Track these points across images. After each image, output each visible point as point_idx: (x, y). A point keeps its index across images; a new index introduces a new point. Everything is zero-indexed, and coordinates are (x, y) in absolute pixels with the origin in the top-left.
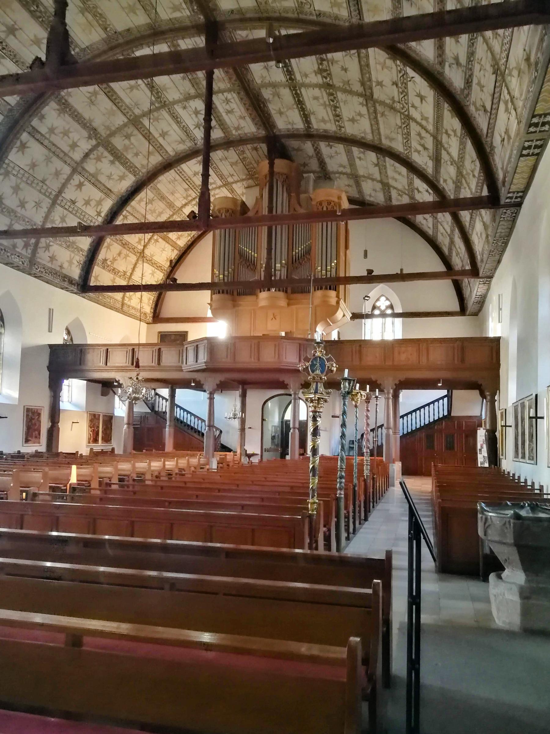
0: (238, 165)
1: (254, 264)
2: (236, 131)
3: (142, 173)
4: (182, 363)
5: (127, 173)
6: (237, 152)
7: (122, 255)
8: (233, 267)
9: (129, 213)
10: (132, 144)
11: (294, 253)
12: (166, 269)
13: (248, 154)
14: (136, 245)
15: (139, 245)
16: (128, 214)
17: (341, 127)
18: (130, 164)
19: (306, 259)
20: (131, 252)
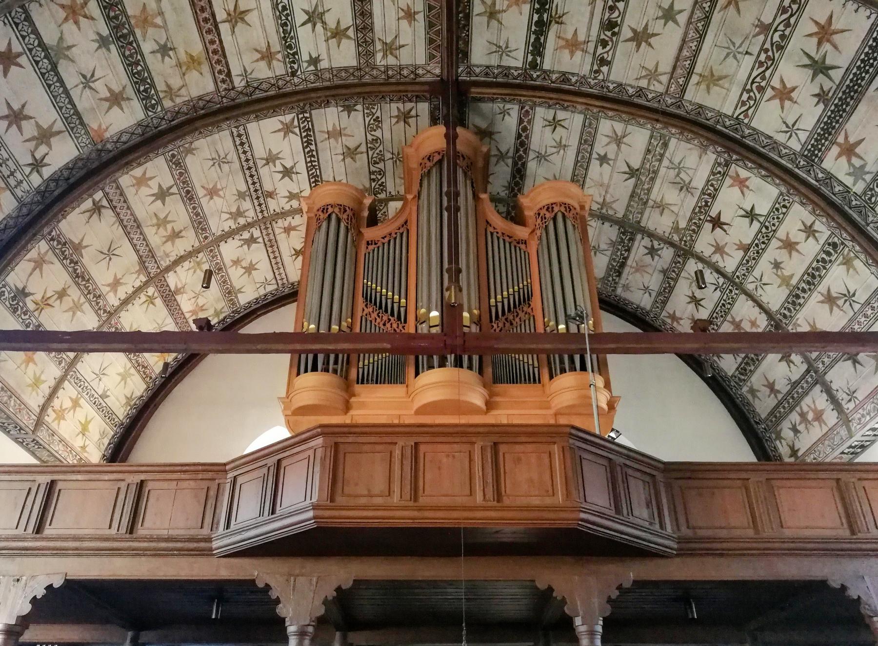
2: (385, 56)
3: (163, 108)
4: (214, 526)
5: (130, 92)
6: (367, 120)
7: (67, 302)
9: (110, 201)
10: (161, 13)
11: (493, 301)
12: (154, 377)
13: (385, 132)
14: (105, 290)
15: (111, 294)
16: (105, 203)
17: (603, 62)
18: (143, 70)
19: (521, 314)
20: (90, 301)
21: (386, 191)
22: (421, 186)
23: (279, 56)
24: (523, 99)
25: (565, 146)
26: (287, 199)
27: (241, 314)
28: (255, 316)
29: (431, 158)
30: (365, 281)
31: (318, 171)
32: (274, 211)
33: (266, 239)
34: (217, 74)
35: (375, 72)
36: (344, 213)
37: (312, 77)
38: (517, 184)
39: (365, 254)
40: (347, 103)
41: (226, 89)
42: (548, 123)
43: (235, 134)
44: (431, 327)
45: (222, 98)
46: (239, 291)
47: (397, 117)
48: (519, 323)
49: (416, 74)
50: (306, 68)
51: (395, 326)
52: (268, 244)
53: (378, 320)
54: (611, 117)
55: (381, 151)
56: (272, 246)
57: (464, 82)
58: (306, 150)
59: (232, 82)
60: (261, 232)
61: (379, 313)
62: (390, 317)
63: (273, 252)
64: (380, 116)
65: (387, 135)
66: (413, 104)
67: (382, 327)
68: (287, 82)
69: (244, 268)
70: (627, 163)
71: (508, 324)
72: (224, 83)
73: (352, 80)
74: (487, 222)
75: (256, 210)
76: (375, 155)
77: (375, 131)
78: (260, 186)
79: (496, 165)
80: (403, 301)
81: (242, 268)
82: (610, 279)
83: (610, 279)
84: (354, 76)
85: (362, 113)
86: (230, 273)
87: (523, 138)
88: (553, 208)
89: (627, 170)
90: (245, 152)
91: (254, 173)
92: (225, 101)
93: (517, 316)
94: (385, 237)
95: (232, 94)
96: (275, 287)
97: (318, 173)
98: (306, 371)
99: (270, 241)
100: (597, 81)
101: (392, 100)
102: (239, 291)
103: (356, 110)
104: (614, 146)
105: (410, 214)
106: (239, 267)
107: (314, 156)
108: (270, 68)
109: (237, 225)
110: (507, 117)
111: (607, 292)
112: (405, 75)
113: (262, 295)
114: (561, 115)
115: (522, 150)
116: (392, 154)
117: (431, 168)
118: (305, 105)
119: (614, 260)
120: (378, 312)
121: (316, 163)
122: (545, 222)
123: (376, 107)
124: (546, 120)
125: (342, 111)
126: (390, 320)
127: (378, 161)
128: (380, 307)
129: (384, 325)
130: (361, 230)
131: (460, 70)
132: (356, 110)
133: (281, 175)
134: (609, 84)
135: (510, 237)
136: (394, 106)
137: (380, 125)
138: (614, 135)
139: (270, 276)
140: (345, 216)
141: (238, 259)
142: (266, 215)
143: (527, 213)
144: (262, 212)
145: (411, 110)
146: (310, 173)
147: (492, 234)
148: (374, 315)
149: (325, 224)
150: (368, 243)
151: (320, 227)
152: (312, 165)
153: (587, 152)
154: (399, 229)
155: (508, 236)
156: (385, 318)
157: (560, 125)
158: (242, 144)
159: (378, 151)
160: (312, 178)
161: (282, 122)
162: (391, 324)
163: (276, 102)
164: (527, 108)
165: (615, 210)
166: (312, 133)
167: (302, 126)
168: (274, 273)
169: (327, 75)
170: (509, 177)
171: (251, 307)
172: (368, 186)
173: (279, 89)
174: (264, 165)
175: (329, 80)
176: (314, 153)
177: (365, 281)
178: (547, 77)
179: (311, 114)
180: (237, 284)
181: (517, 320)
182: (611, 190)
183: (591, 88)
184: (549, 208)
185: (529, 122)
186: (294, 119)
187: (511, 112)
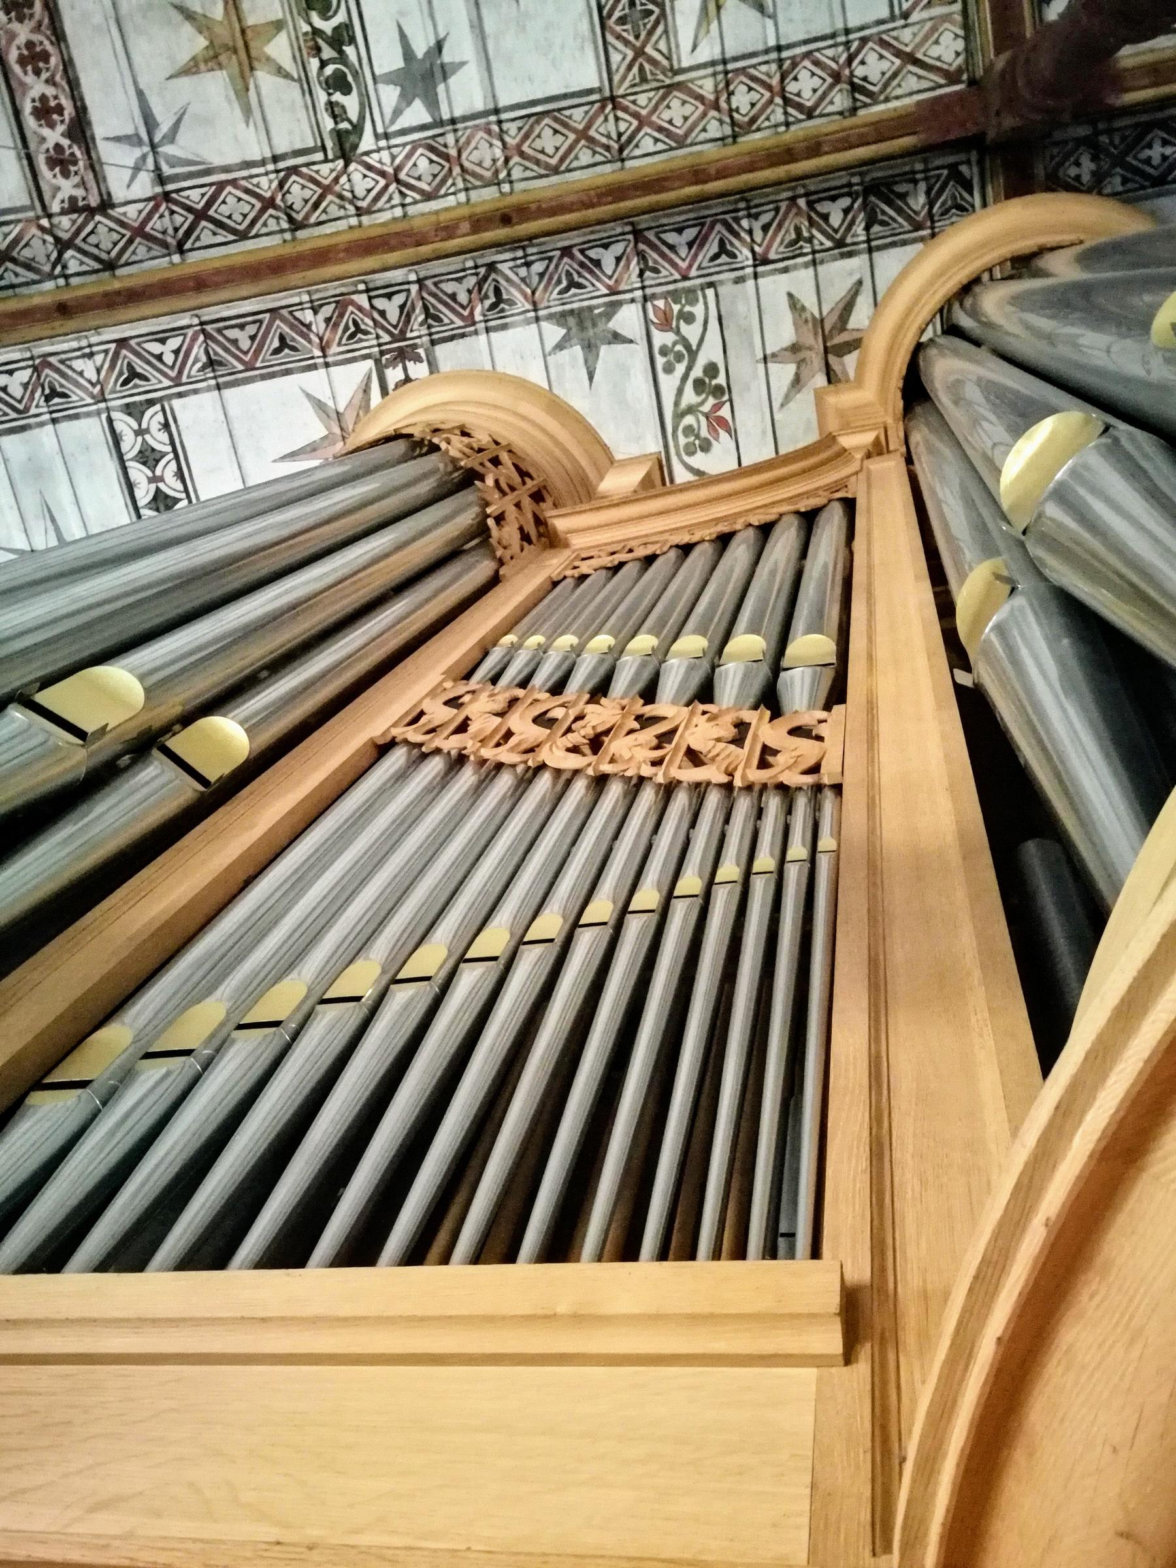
6: (669, 384)
23: (280, 49)
34: (30, 122)
37: (423, 164)
40: (577, 301)
41: (73, 207)
43: (130, 445)
45: (63, 245)
49: (854, 88)
50: (397, 113)
59: (95, 166)
66: (857, 265)
68: (327, 190)
72: (66, 174)
77: (706, 447)
85: (641, 349)
92: (73, 267)
95: (104, 234)
101: (766, 261)
103: (617, 338)
108: (247, 112)
112: (808, 99)
125: (560, 347)
132: (617, 338)
136: (775, 286)
137: (725, 412)
145: (848, 307)
173: (296, 226)
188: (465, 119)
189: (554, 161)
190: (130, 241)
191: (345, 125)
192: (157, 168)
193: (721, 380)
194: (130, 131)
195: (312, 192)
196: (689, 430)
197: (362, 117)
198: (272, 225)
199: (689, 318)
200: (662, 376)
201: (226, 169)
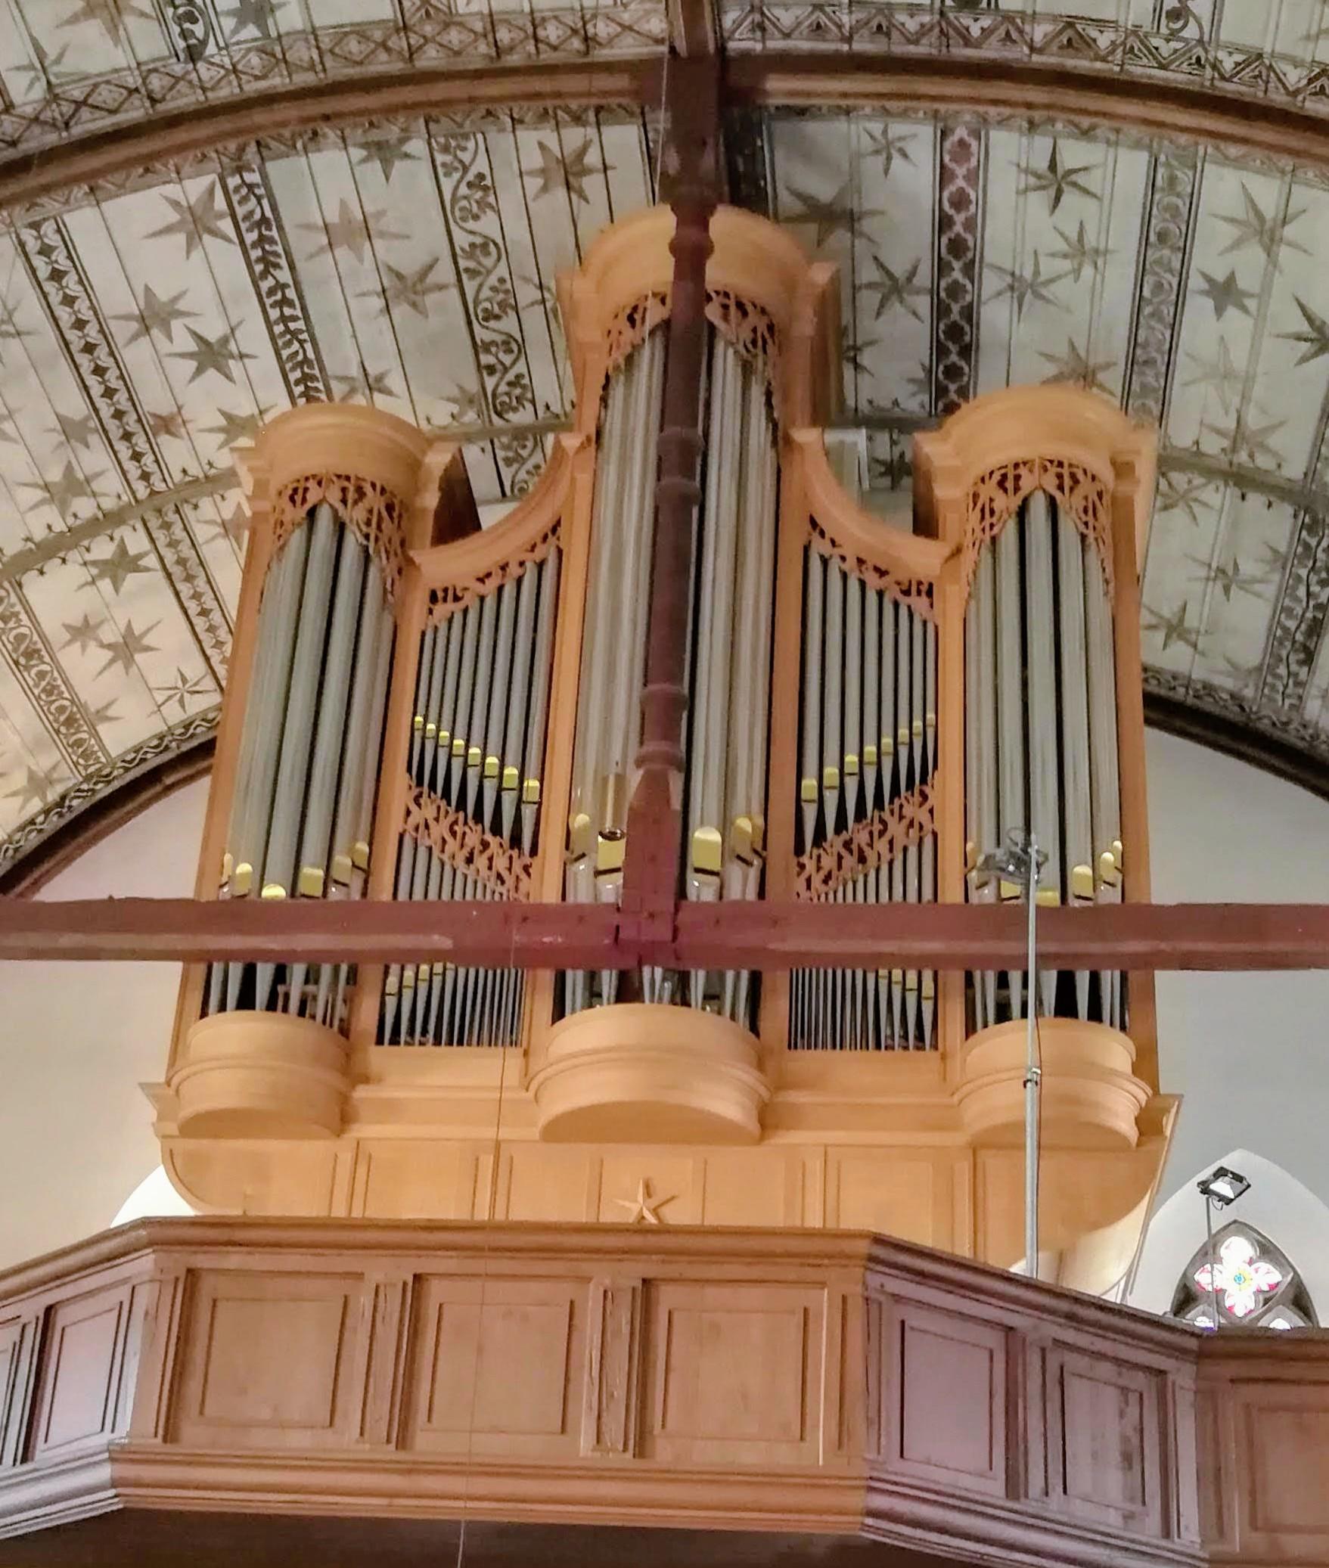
0: (430, 300)
1: (516, 841)
6: (447, 186)
8: (363, 847)
11: (810, 783)
19: (896, 828)
21: (533, 402)
22: (604, 400)
24: (942, 107)
25: (1097, 251)
26: (222, 437)
27: (116, 785)
28: (159, 788)
29: (638, 317)
30: (419, 719)
31: (308, 346)
32: (184, 471)
33: (170, 557)
35: (454, 37)
36: (355, 502)
37: (255, 60)
38: (953, 372)
39: (423, 634)
40: (375, 135)
42: (1032, 181)
44: (598, 873)
46: (102, 715)
47: (543, 172)
48: (886, 856)
50: (235, 32)
51: (500, 864)
52: (177, 571)
53: (452, 845)
54: (1236, 160)
55: (502, 280)
56: (189, 578)
57: (746, 56)
58: (266, 285)
60: (152, 540)
61: (456, 822)
62: (488, 837)
63: (197, 596)
64: (487, 172)
65: (516, 230)
67: (461, 867)
68: (177, 80)
69: (109, 647)
70: (1303, 308)
71: (849, 861)
73: (383, 64)
74: (814, 523)
75: (124, 473)
76: (486, 293)
77: (476, 217)
78: (131, 399)
79: (879, 314)
80: (532, 783)
81: (102, 646)
82: (1282, 670)
83: (1282, 670)
84: (388, 50)
86: (63, 663)
87: (958, 228)
88: (1017, 478)
89: (1305, 328)
90: (69, 301)
91: (105, 361)
93: (881, 834)
94: (489, 575)
96: (216, 698)
97: (311, 355)
98: (222, 1007)
99: (182, 562)
100: (1179, 45)
101: (521, 122)
102: (102, 715)
103: (407, 156)
104: (1253, 255)
105: (571, 498)
106: (92, 646)
107: (291, 304)
108: (117, 41)
109: (70, 521)
110: (897, 161)
111: (1276, 712)
113: (176, 726)
114: (1074, 153)
115: (957, 265)
116: (541, 287)
117: (636, 348)
118: (242, 149)
119: (1289, 612)
120: (451, 818)
121: (300, 324)
122: (992, 526)
123: (471, 145)
124: (1027, 171)
125: (364, 160)
126: (485, 845)
127: (496, 310)
128: (461, 805)
129: (469, 860)
130: (411, 553)
131: (728, 21)
132: (407, 156)
133: (192, 365)
134: (1221, 55)
135: (882, 573)
136: (529, 138)
138: (1255, 222)
139: (195, 668)
140: (359, 513)
141: (86, 619)
142: (160, 486)
143: (947, 493)
144: (145, 476)
146: (285, 353)
147: (825, 562)
148: (440, 830)
149: (297, 538)
150: (433, 598)
151: (282, 548)
152: (287, 330)
153: (1171, 271)
154: (533, 548)
155: (877, 569)
156: (473, 840)
157: (1074, 184)
158: (57, 275)
159: (493, 280)
160: (293, 369)
161: (175, 204)
162: (491, 859)
163: (145, 146)
164: (961, 132)
165: (1275, 454)
166: (274, 233)
167: (240, 211)
168: (207, 659)
169: (301, 53)
170: (923, 351)
171: (143, 760)
172: (473, 387)
174: (135, 337)
175: (312, 67)
176: (291, 293)
177: (419, 719)
178: (1014, 35)
179: (264, 176)
180: (91, 695)
181: (882, 845)
182: (1258, 391)
183: (1162, 67)
184: (1007, 479)
185: (972, 177)
186: (211, 192)
187: (910, 148)
188: (288, 34)
189: (358, 59)
190: (28, 127)
191: (193, 41)
192: (49, 82)
193: (488, 182)
194: (26, 62)
195: (168, 81)
196: (462, 209)
197: (206, 34)
198: (137, 103)
199: (464, 149)
200: (442, 179)
201: (100, 75)
